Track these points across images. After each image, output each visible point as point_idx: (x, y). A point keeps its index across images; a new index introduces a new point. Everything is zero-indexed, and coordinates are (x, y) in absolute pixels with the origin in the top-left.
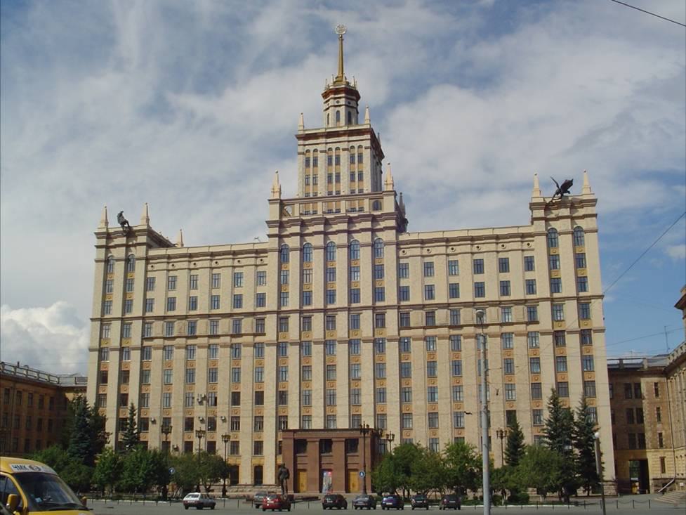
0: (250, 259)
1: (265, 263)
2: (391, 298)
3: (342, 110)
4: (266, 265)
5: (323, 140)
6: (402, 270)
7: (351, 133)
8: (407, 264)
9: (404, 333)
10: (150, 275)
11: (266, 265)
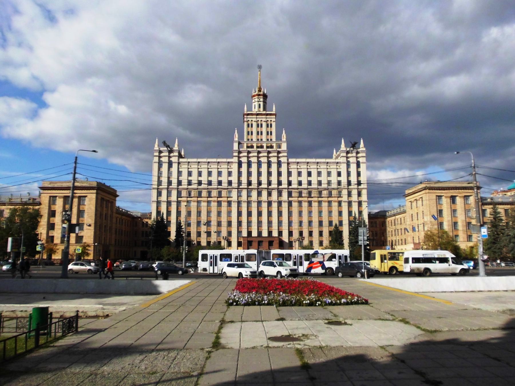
2: (285, 185)
3: (262, 104)
5: (255, 117)
6: (289, 174)
7: (267, 115)
9: (290, 199)
10: (180, 170)
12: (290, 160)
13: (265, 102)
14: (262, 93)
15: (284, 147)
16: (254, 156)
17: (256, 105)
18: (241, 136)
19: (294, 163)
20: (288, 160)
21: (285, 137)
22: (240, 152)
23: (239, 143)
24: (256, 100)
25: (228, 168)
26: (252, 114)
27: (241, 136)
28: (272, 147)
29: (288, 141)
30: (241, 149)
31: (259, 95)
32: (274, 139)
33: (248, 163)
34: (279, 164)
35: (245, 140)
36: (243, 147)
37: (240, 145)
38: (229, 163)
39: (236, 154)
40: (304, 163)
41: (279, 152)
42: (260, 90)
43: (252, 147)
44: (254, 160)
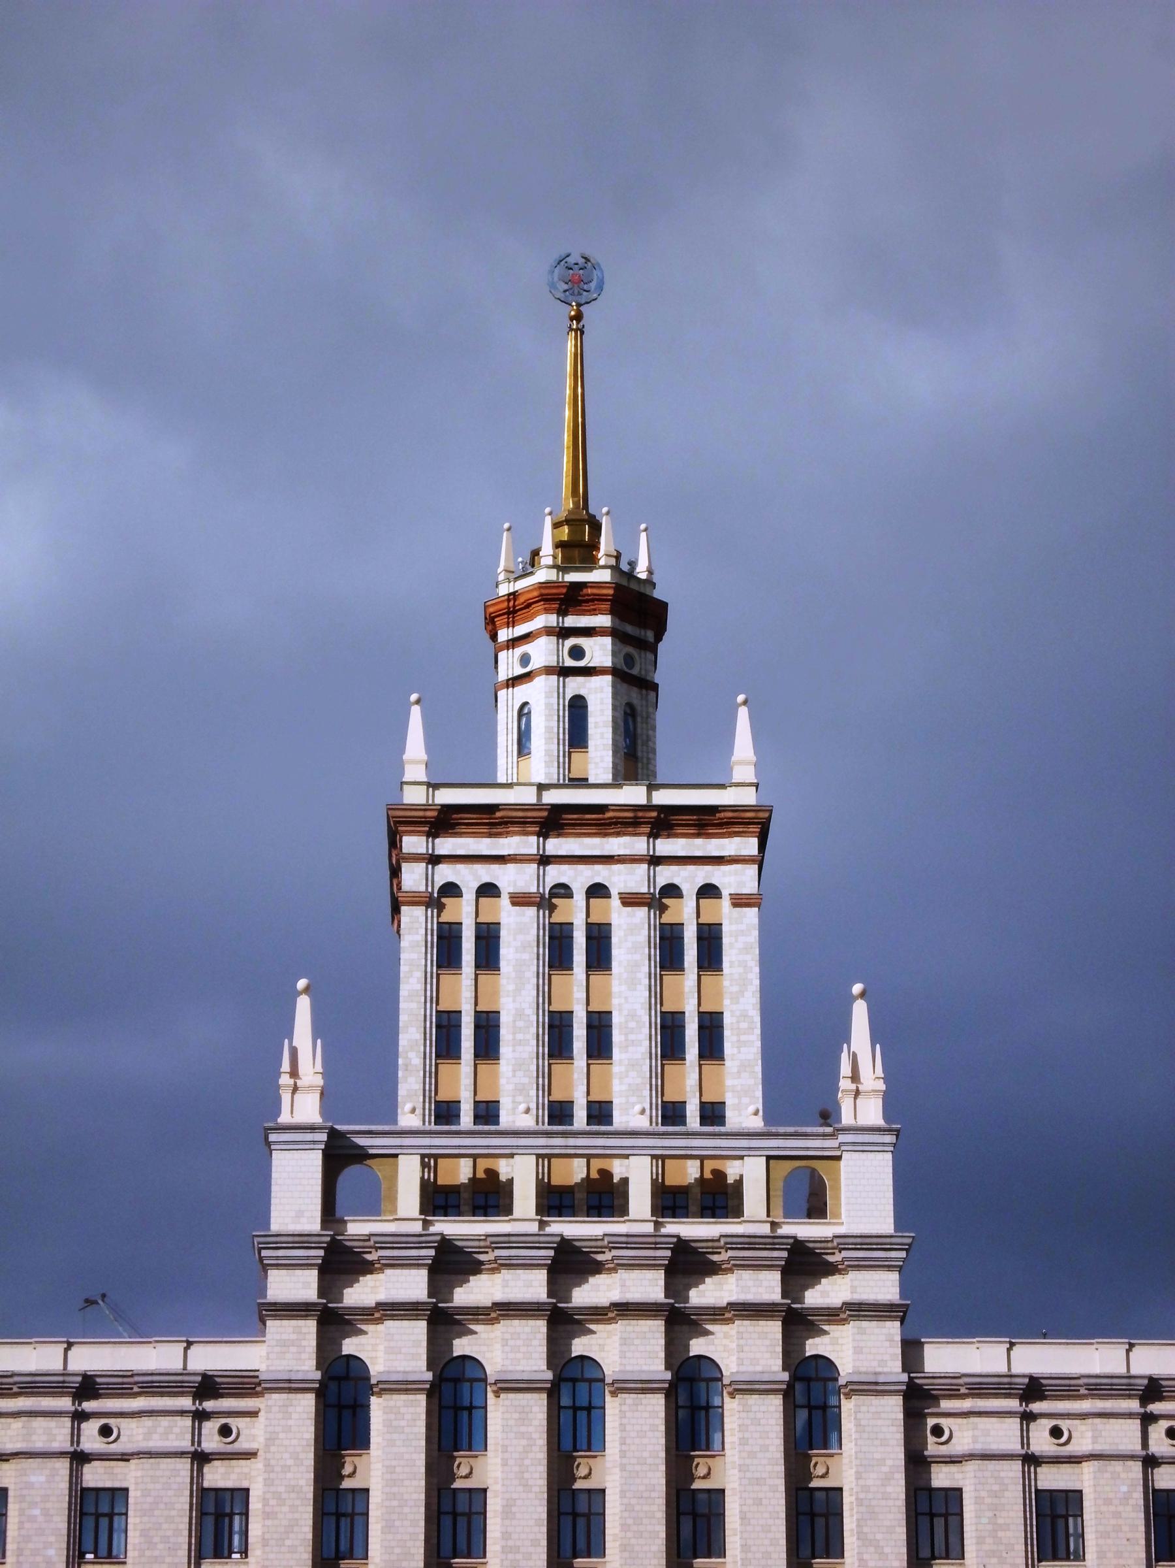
0: (165, 1421)
1: (243, 1445)
3: (600, 695)
4: (250, 1455)
5: (527, 844)
7: (664, 821)
8: (954, 1495)
11: (250, 1455)
12: (944, 1358)
13: (635, 683)
14: (602, 575)
15: (865, 1197)
16: (625, 1310)
17: (536, 724)
18: (362, 1070)
19: (981, 1387)
20: (911, 1351)
21: (872, 1078)
22: (341, 1262)
23: (340, 1156)
24: (542, 652)
25: (201, 1458)
26: (490, 819)
27: (362, 1070)
28: (719, 1197)
29: (910, 1135)
30: (357, 1228)
31: (569, 599)
32: (745, 1109)
33: (434, 1392)
34: (811, 1402)
35: (411, 1113)
36: (376, 1202)
37: (350, 1176)
38: (208, 1386)
39: (300, 1285)
40: (1100, 1387)
41: (804, 1264)
42: (579, 546)
43: (490, 1196)
44: (510, 1351)
